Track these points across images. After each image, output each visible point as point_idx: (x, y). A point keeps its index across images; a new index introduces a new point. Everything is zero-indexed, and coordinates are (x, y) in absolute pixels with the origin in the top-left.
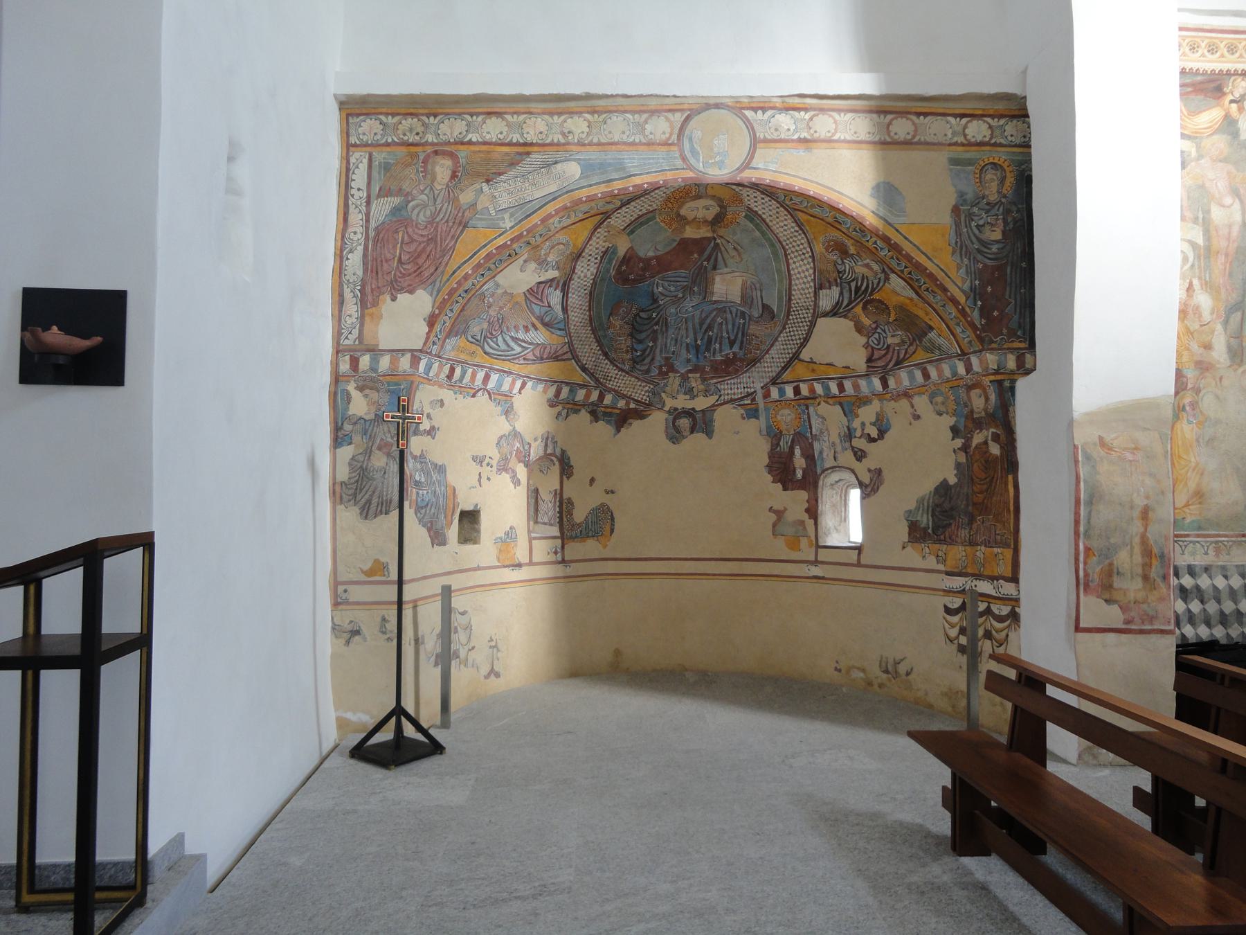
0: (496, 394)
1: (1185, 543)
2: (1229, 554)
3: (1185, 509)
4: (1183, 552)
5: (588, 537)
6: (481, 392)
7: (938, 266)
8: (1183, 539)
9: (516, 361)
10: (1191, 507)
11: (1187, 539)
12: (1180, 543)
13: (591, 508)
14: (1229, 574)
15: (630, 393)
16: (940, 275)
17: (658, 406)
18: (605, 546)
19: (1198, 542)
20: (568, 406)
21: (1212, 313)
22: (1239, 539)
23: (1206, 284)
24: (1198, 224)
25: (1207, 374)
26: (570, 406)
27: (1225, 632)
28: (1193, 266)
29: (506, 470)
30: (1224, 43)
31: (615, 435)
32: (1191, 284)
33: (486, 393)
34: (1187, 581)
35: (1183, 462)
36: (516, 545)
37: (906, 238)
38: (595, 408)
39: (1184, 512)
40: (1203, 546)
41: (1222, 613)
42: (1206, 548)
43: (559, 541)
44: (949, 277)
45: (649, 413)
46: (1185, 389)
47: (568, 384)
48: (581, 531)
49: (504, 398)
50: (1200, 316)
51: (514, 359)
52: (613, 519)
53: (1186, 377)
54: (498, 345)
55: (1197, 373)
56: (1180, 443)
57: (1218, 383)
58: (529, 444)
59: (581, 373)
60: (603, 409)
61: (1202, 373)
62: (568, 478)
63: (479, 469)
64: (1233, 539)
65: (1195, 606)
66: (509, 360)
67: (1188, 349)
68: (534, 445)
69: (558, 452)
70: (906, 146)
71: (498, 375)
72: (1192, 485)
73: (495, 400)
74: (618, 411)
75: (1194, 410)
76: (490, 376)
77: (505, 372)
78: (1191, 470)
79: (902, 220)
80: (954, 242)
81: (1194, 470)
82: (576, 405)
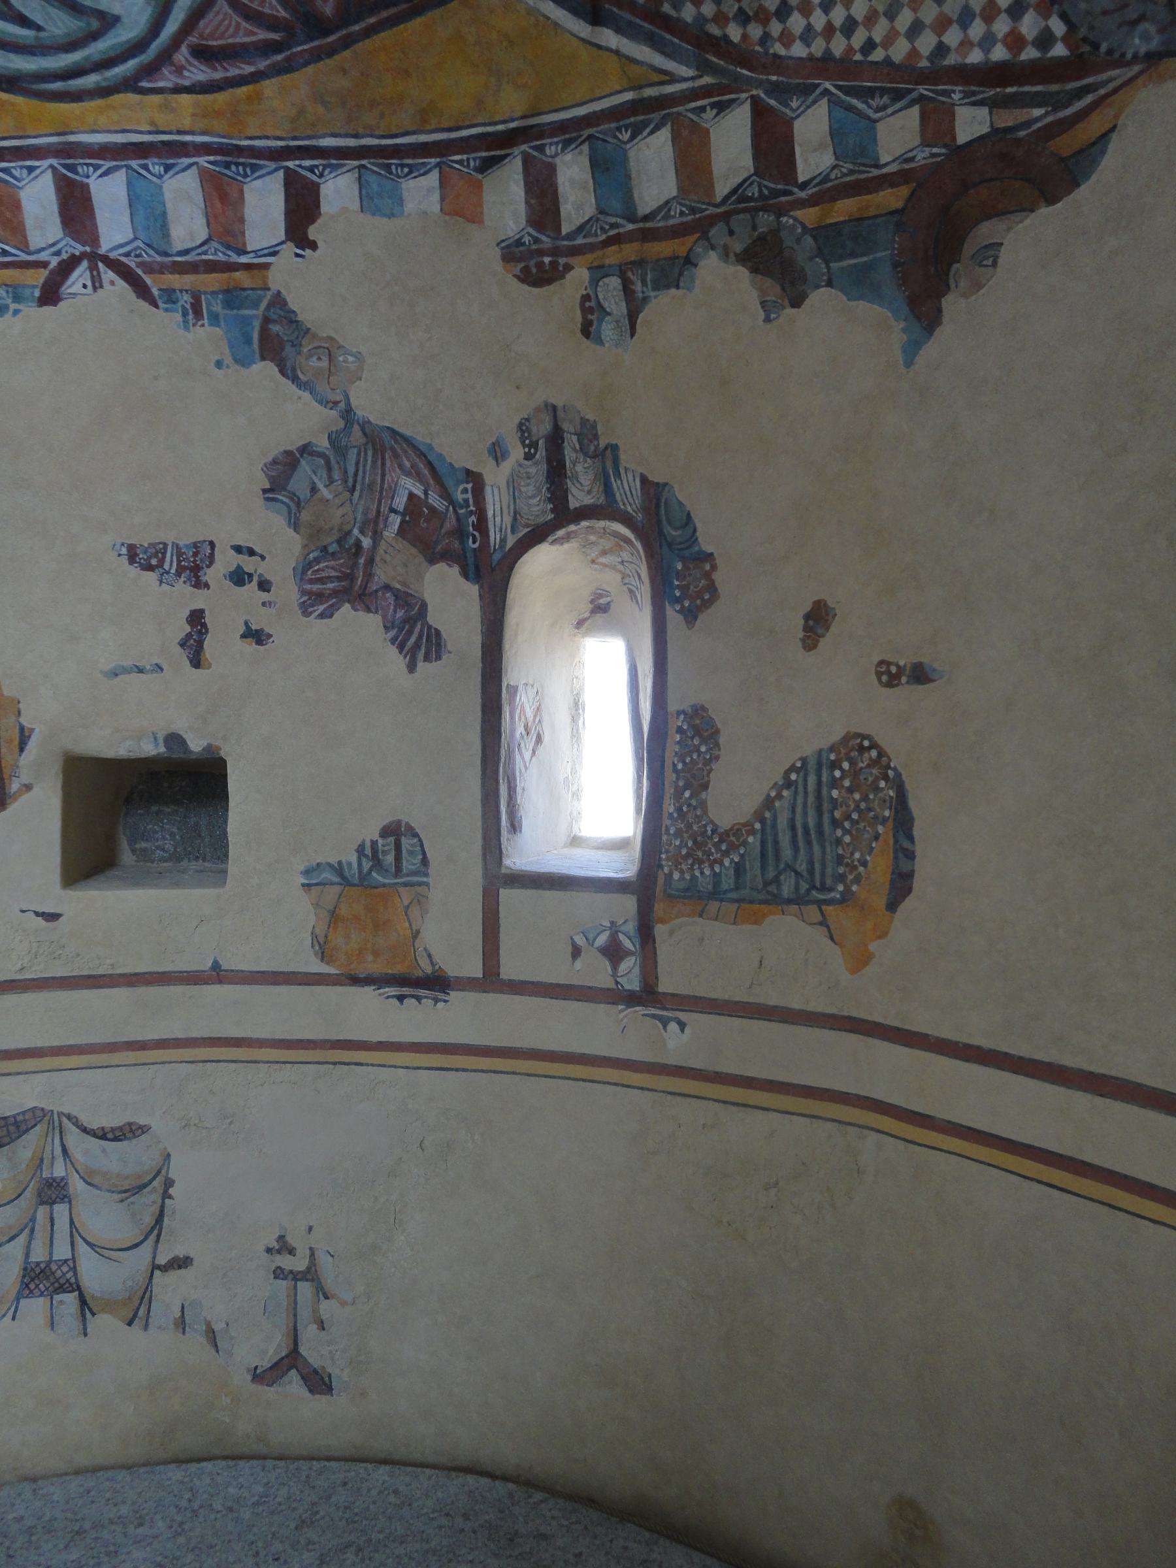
0: (162, 269)
5: (775, 901)
6: (80, 274)
9: (166, 79)
13: (793, 758)
15: (926, 43)
17: (1138, 44)
18: (860, 960)
20: (612, 256)
26: (630, 251)
29: (363, 598)
31: (911, 351)
33: (108, 275)
36: (420, 901)
38: (766, 220)
43: (630, 903)
45: (1095, 125)
47: (568, 132)
48: (739, 869)
49: (212, 281)
51: (150, 70)
52: (903, 821)
54: (23, 21)
58: (476, 480)
59: (582, 28)
60: (810, 216)
62: (690, 616)
63: (186, 598)
66: (129, 85)
68: (496, 478)
69: (629, 493)
71: (120, 177)
73: (170, 295)
74: (892, 198)
76: (85, 188)
77: (141, 150)
82: (647, 235)
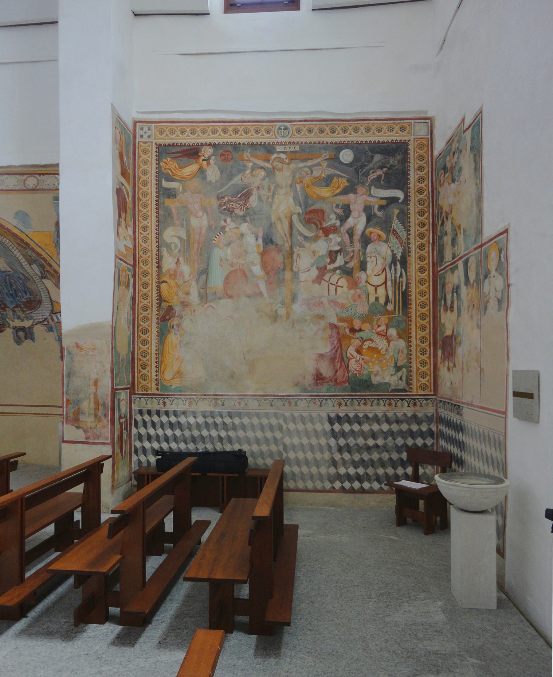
1: (173, 399)
2: (197, 405)
3: (172, 381)
4: (172, 403)
7: (47, 253)
8: (171, 397)
10: (175, 380)
11: (173, 397)
12: (170, 399)
14: (196, 415)
16: (48, 259)
19: (180, 398)
21: (190, 276)
22: (203, 397)
23: (187, 259)
24: (183, 228)
25: (187, 308)
27: (195, 446)
28: (180, 250)
30: (179, 128)
32: (178, 260)
34: (173, 419)
35: (171, 356)
37: (31, 240)
39: (171, 382)
40: (183, 400)
41: (193, 436)
42: (184, 401)
44: (53, 259)
46: (175, 316)
50: (184, 277)
53: (175, 310)
55: (181, 308)
56: (170, 345)
57: (193, 313)
61: (184, 308)
64: (199, 397)
65: (178, 433)
67: (177, 295)
70: (32, 192)
72: (175, 368)
75: (178, 327)
78: (175, 360)
79: (29, 230)
80: (56, 241)
81: (177, 360)
